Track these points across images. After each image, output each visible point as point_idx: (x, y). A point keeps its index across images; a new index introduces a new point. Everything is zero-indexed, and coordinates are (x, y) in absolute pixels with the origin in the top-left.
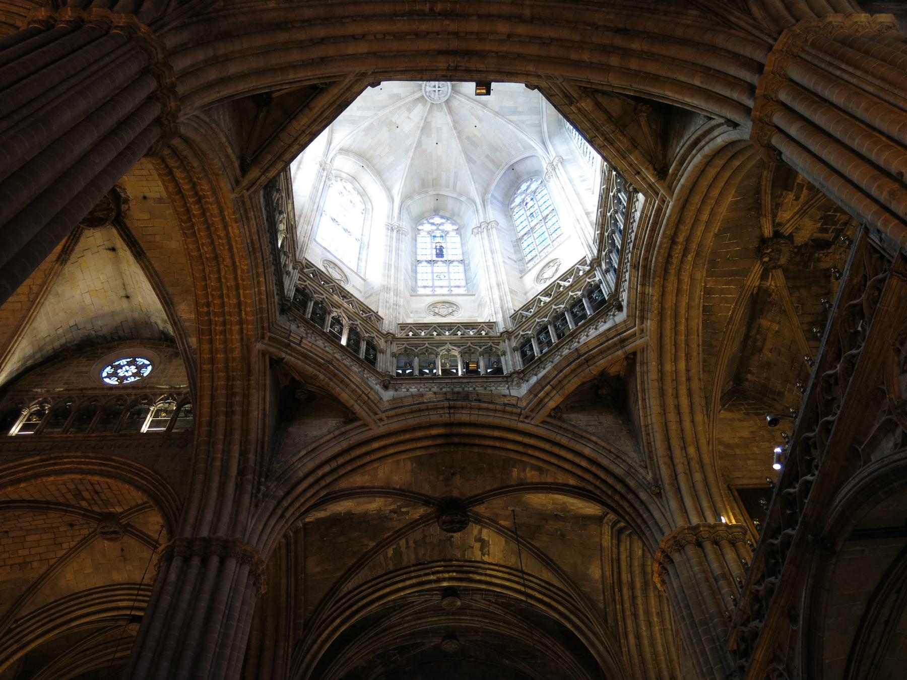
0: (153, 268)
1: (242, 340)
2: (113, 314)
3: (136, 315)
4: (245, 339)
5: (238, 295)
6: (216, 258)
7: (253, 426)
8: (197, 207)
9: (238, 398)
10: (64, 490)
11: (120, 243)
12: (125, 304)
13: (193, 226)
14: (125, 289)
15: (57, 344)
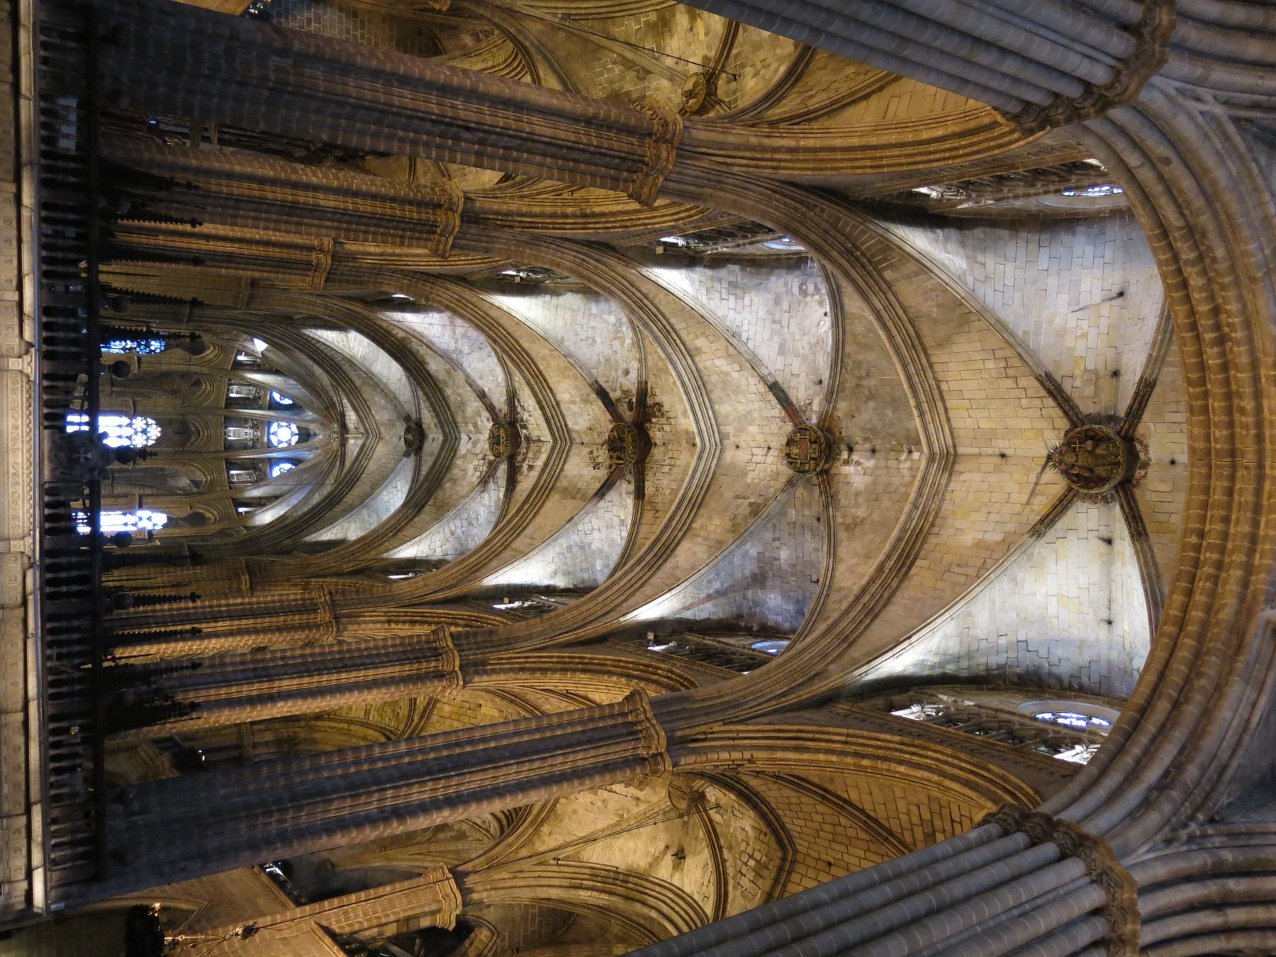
0: (1153, 556)
1: (1242, 598)
2: (1082, 644)
3: (1114, 655)
4: (1249, 597)
5: (1256, 524)
6: (1233, 454)
7: (1214, 731)
8: (1216, 350)
9: (1203, 682)
10: (915, 820)
11: (1121, 531)
12: (1102, 632)
13: (1206, 395)
14: (1109, 608)
15: (994, 660)
